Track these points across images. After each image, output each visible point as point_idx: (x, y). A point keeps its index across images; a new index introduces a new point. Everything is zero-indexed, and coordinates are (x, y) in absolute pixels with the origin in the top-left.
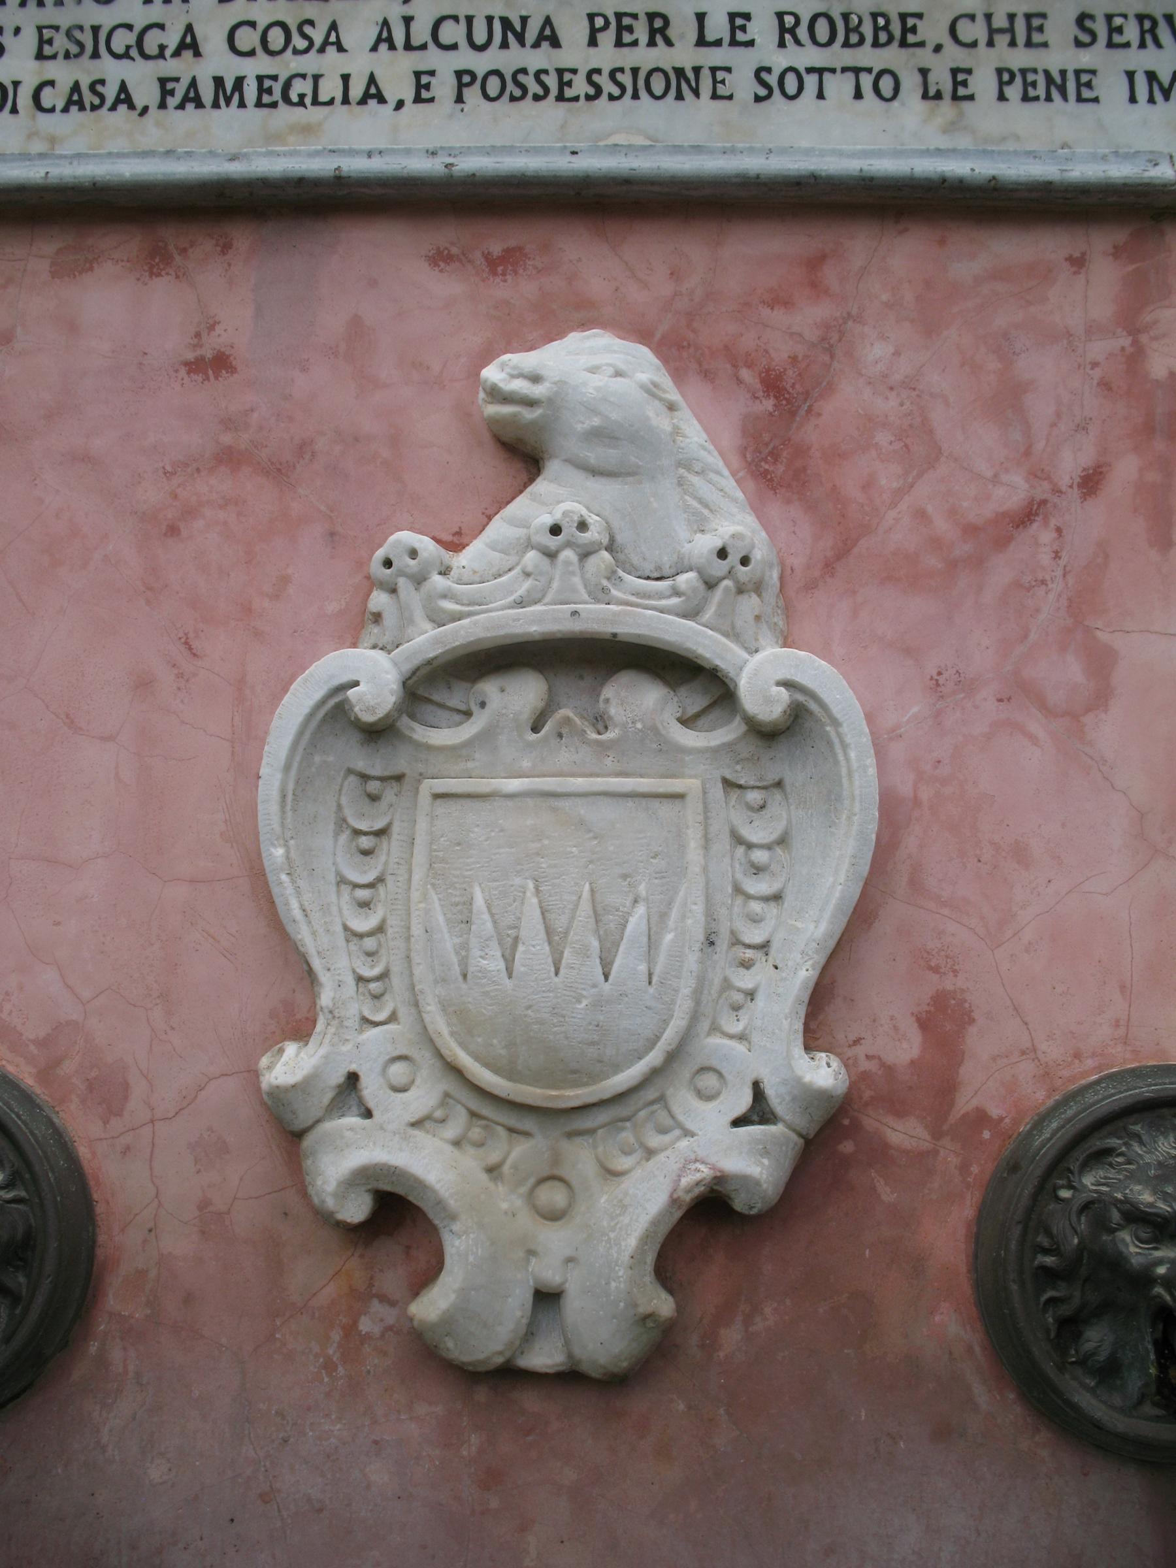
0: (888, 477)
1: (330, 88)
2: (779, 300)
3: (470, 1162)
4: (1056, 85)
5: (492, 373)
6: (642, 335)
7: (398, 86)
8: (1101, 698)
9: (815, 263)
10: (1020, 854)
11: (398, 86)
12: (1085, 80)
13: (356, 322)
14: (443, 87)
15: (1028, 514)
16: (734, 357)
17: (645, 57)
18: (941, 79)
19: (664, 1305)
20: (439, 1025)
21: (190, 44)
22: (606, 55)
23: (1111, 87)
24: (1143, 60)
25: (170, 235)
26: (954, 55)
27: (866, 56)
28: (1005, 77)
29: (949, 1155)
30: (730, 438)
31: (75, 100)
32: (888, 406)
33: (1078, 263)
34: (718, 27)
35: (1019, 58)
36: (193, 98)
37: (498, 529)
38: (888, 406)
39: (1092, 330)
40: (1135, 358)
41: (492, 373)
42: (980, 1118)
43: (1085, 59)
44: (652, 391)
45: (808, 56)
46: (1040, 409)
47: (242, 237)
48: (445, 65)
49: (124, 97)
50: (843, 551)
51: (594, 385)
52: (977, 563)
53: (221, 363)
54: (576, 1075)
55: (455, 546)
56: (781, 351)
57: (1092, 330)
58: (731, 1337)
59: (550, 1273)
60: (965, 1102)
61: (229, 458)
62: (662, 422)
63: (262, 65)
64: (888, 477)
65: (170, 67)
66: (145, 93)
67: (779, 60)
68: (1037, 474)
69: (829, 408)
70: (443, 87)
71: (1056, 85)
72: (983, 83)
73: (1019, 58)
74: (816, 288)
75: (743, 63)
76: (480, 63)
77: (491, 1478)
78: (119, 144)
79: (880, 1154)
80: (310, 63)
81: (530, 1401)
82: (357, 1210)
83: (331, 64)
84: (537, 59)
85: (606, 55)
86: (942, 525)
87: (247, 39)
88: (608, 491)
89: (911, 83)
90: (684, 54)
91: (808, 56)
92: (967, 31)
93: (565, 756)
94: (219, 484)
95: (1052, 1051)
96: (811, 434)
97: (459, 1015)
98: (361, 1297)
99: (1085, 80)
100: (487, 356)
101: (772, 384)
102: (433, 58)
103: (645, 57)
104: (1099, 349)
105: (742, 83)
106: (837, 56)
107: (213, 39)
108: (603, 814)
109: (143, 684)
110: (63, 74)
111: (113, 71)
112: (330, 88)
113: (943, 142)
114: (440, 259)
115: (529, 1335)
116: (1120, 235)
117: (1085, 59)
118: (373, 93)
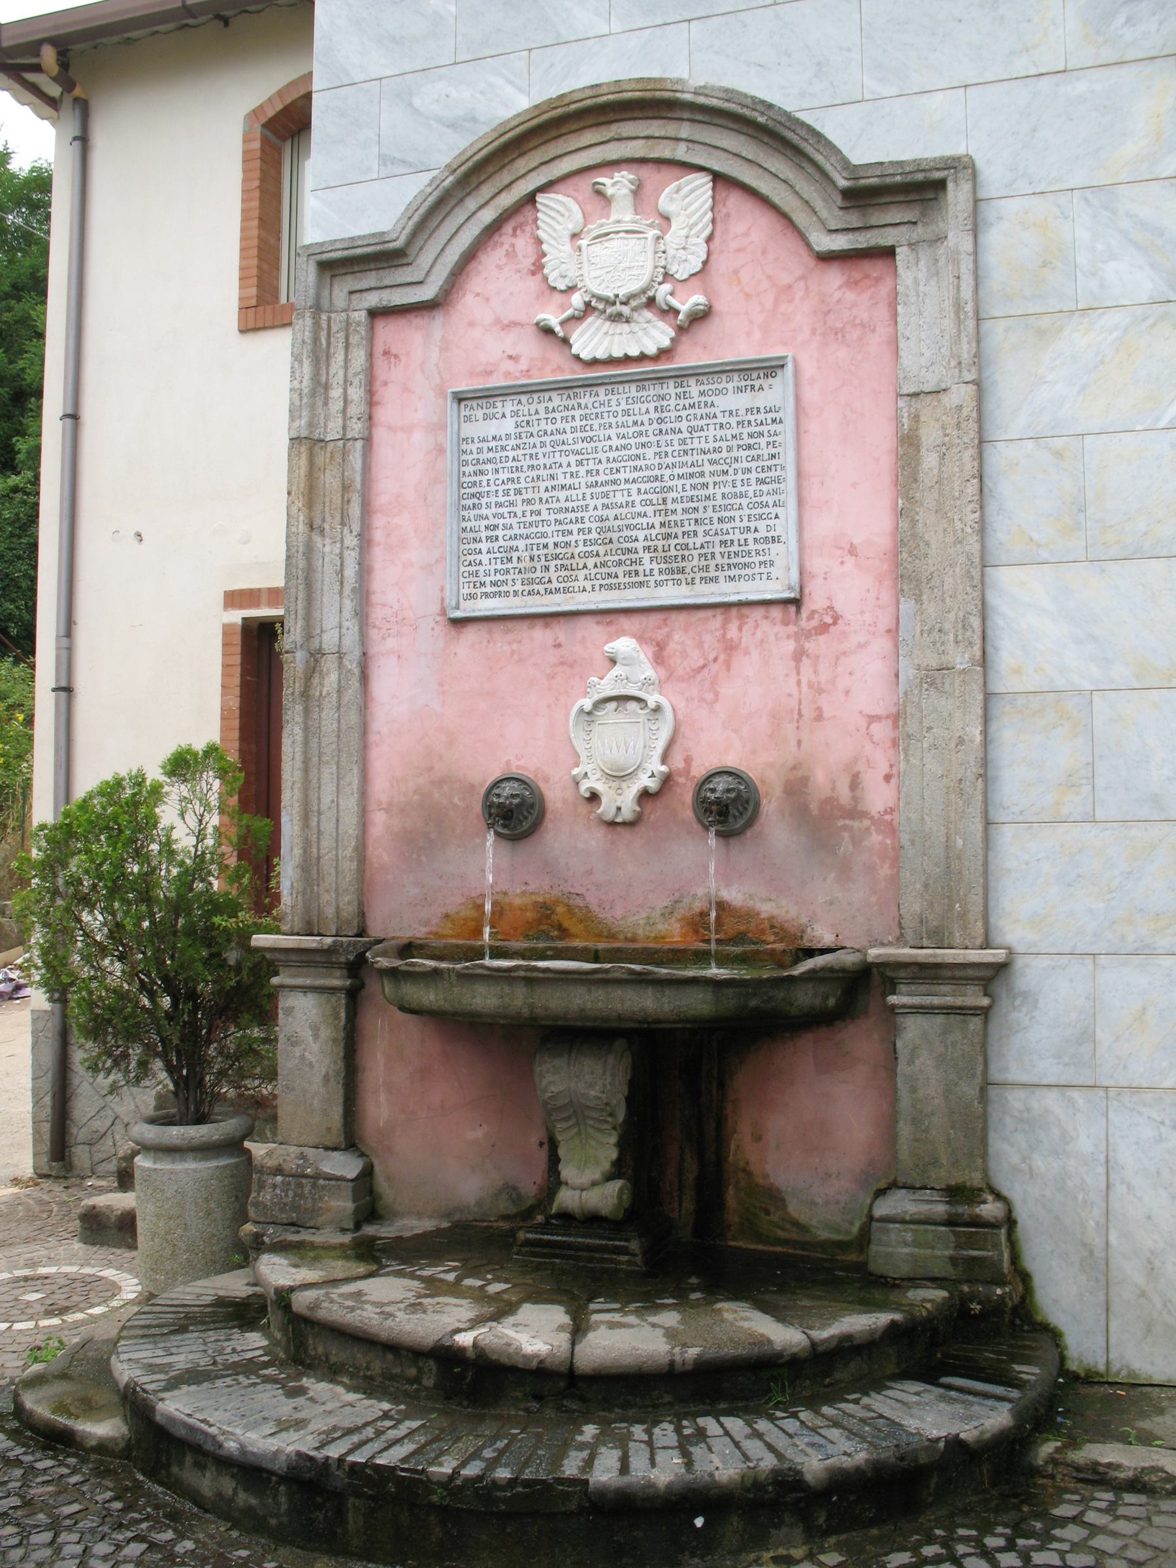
0: (679, 661)
1: (576, 589)
2: (659, 628)
3: (606, 786)
4: (711, 580)
5: (606, 648)
6: (634, 636)
7: (589, 588)
8: (717, 700)
9: (665, 620)
10: (702, 730)
11: (589, 588)
12: (717, 578)
13: (584, 638)
14: (597, 588)
15: (704, 667)
16: (651, 639)
17: (634, 579)
18: (689, 580)
19: (638, 809)
20: (601, 764)
21: (550, 581)
22: (627, 580)
23: (722, 579)
24: (728, 573)
25: (548, 620)
26: (692, 575)
27: (676, 576)
28: (702, 579)
29: (689, 783)
30: (650, 655)
31: (529, 593)
32: (679, 647)
33: (714, 616)
34: (648, 572)
35: (705, 574)
36: (551, 592)
37: (608, 676)
38: (679, 647)
39: (717, 630)
40: (724, 635)
41: (606, 648)
42: (694, 777)
43: (717, 574)
44: (634, 649)
45: (664, 577)
46: (706, 646)
47: (562, 620)
48: (597, 583)
49: (538, 593)
50: (671, 675)
51: (623, 649)
52: (694, 676)
53: (559, 646)
54: (622, 770)
55: (602, 679)
56: (659, 638)
57: (717, 630)
58: (652, 817)
59: (619, 804)
60: (692, 774)
61: (562, 664)
62: (635, 654)
63: (563, 585)
64: (679, 661)
65: (546, 586)
66: (543, 592)
67: (659, 578)
68: (705, 659)
69: (668, 649)
70: (597, 588)
71: (711, 580)
72: (697, 581)
73: (705, 574)
74: (666, 625)
75: (652, 579)
76: (604, 582)
77: (613, 843)
78: (538, 603)
79: (678, 784)
80: (572, 584)
81: (619, 829)
82: (587, 795)
83: (576, 584)
84: (614, 581)
85: (627, 580)
86: (688, 670)
87: (561, 579)
88: (626, 668)
89: (684, 581)
90: (641, 578)
91: (664, 577)
92: (696, 569)
93: (621, 716)
94: (560, 669)
95: (707, 764)
96: (665, 653)
97: (605, 763)
98: (591, 812)
99: (717, 578)
100: (607, 642)
101: (658, 644)
102: (595, 582)
103: (634, 579)
104: (717, 634)
105: (652, 584)
106: (670, 577)
107: (554, 580)
108: (626, 726)
109: (549, 706)
110: (527, 588)
111: (536, 587)
112: (576, 589)
113: (689, 594)
114: (598, 623)
115: (616, 815)
116: (722, 610)
117: (717, 574)
118: (584, 590)
